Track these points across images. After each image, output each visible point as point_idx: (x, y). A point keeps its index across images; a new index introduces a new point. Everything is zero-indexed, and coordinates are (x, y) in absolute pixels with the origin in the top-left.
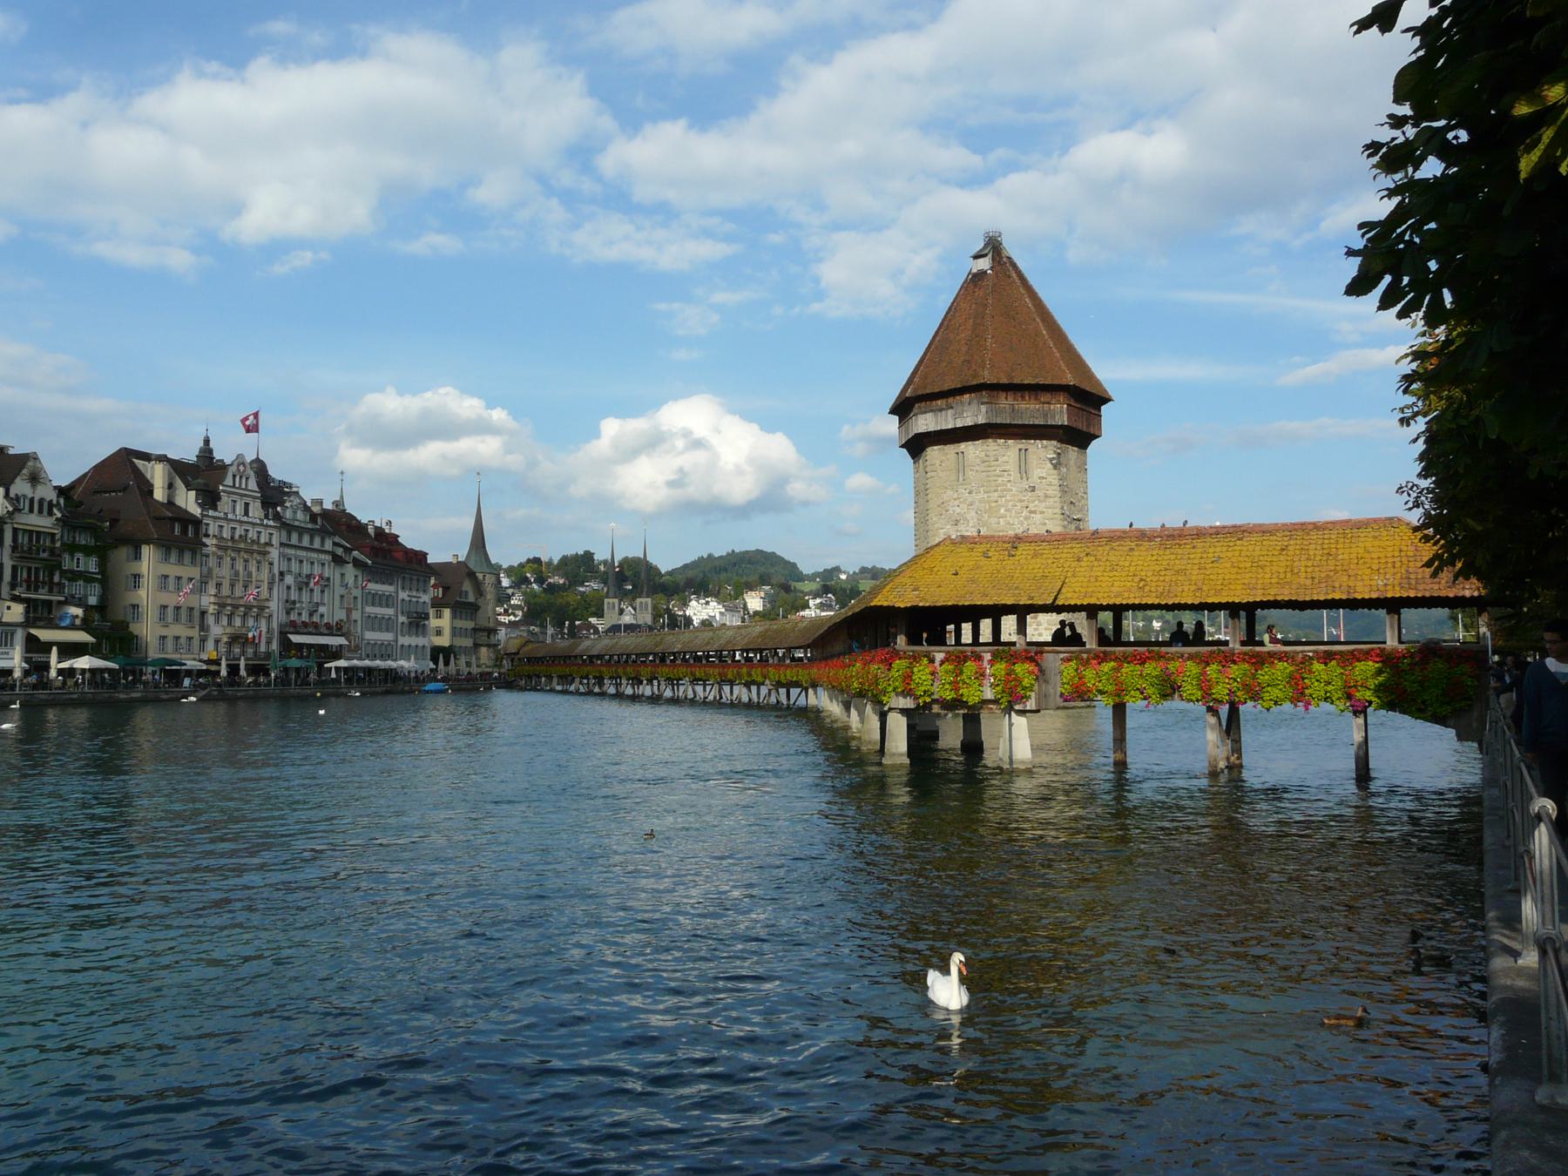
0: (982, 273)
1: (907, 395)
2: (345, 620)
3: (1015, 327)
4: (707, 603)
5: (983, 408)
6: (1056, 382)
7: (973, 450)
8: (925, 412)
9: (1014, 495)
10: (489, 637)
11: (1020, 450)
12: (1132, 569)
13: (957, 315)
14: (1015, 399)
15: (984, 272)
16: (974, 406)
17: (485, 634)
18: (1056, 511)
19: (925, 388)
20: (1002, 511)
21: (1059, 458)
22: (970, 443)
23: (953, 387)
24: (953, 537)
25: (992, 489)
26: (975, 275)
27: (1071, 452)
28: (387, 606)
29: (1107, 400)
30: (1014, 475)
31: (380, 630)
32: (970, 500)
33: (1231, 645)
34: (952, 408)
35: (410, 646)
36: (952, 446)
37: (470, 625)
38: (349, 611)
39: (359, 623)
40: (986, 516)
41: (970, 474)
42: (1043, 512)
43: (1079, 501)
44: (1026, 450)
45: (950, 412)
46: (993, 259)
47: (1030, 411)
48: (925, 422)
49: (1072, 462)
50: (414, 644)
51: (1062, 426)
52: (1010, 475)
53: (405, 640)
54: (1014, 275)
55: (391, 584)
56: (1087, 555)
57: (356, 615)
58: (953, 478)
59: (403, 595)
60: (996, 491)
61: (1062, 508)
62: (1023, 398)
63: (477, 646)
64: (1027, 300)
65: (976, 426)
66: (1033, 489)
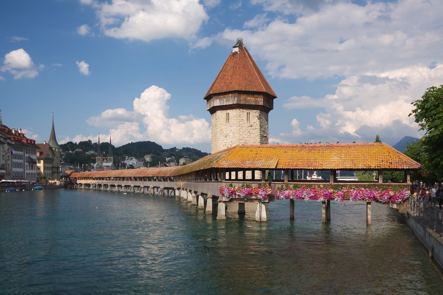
2: (5, 163)
4: (132, 159)
6: (260, 91)
7: (232, 113)
9: (245, 128)
10: (57, 170)
11: (247, 113)
12: (300, 157)
14: (246, 96)
17: (56, 169)
20: (241, 133)
23: (226, 91)
24: (240, 145)
28: (21, 159)
29: (275, 97)
31: (18, 167)
35: (29, 173)
37: (50, 166)
38: (6, 161)
39: (10, 165)
40: (236, 134)
42: (255, 134)
44: (249, 113)
45: (225, 99)
47: (251, 100)
48: (217, 102)
50: (31, 172)
52: (244, 121)
53: (28, 171)
55: (22, 151)
56: (285, 152)
57: (9, 162)
58: (225, 121)
59: (27, 155)
62: (249, 96)
63: (53, 173)
65: (233, 104)
66: (252, 126)
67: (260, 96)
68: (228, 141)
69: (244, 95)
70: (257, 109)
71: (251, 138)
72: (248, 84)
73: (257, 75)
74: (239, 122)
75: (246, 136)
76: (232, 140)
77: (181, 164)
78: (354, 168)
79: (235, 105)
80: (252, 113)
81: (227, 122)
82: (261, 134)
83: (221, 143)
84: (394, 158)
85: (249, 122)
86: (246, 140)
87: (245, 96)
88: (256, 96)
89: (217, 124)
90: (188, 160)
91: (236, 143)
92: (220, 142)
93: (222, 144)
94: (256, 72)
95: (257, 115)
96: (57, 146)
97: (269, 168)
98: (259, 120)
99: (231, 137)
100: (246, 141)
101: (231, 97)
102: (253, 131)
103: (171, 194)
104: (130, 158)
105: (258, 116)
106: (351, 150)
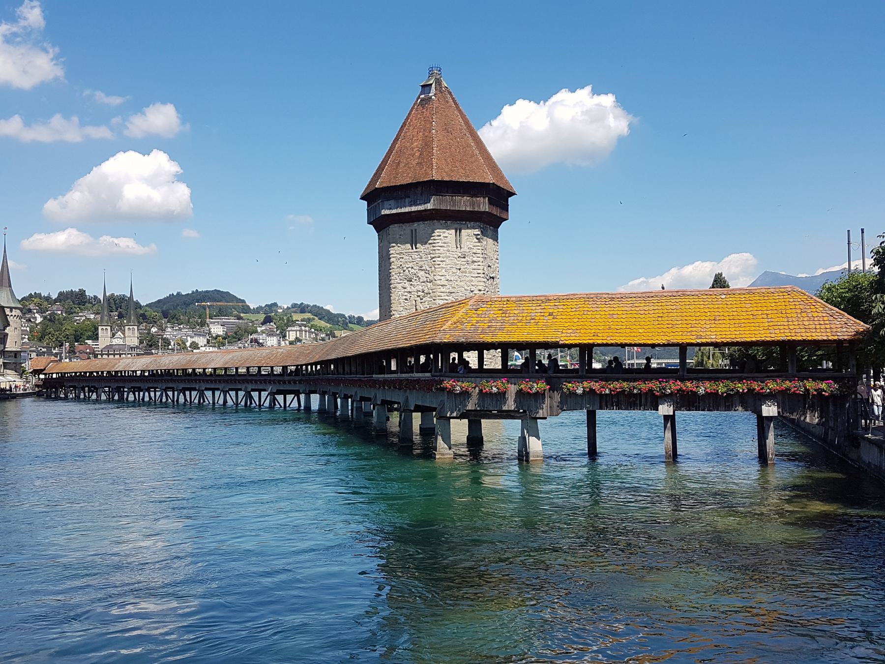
4: (180, 329)
6: (481, 181)
18: (479, 271)
22: (421, 222)
23: (410, 181)
26: (422, 100)
27: (489, 231)
34: (409, 197)
36: (408, 225)
40: (432, 275)
42: (472, 272)
43: (494, 265)
51: (484, 212)
52: (449, 246)
60: (439, 257)
64: (461, 120)
68: (415, 289)
74: (439, 248)
77: (291, 340)
79: (428, 212)
81: (412, 249)
82: (484, 274)
90: (306, 331)
95: (475, 233)
96: (14, 301)
98: (479, 244)
100: (455, 288)
101: (421, 195)
102: (468, 267)
103: (291, 406)
105: (478, 235)
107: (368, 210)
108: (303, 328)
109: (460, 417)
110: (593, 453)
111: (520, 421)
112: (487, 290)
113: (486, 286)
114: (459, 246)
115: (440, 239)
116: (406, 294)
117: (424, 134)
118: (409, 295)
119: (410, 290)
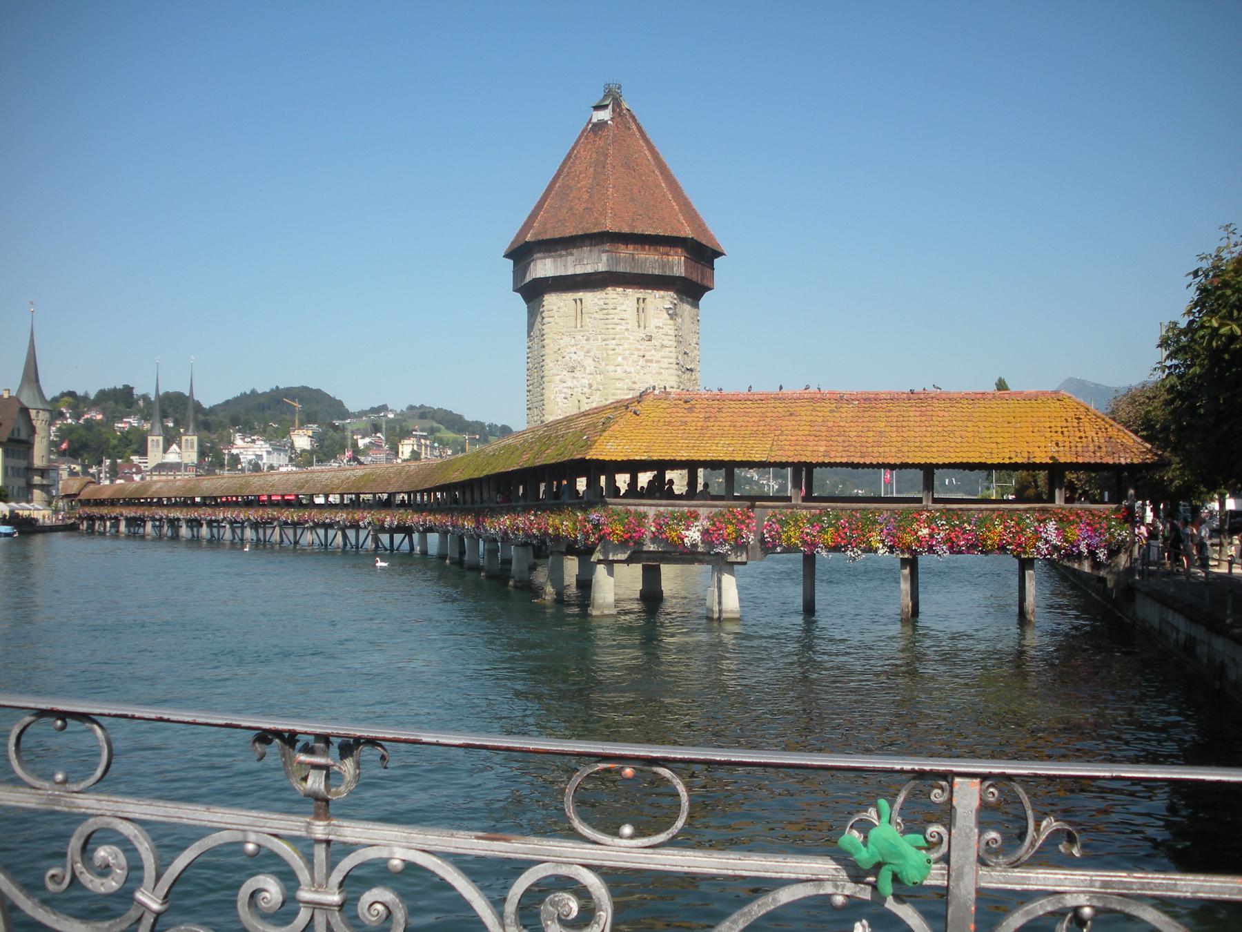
0: (602, 125)
1: (527, 240)
3: (634, 178)
4: (253, 441)
5: (604, 257)
6: (674, 234)
7: (591, 299)
8: (545, 258)
9: (631, 344)
11: (638, 299)
13: (577, 162)
14: (634, 249)
15: (606, 122)
16: (595, 255)
18: (671, 361)
19: (546, 232)
20: (620, 359)
21: (675, 308)
23: (574, 233)
25: (611, 336)
26: (595, 125)
29: (719, 254)
30: (632, 324)
32: (587, 347)
33: (924, 503)
34: (572, 254)
40: (603, 363)
41: (587, 320)
43: (692, 351)
44: (644, 299)
45: (570, 259)
46: (614, 111)
47: (649, 261)
48: (544, 268)
49: (686, 313)
51: (680, 278)
52: (628, 323)
54: (634, 127)
56: (791, 414)
58: (573, 324)
61: (677, 358)
62: (643, 249)
64: (647, 152)
65: (596, 273)
67: (675, 249)
68: (579, 385)
69: (627, 247)
70: (667, 289)
71: (650, 375)
72: (640, 212)
73: (665, 190)
74: (614, 326)
75: (633, 370)
76: (591, 381)
77: (403, 458)
78: (989, 462)
79: (599, 276)
80: (653, 299)
82: (678, 364)
83: (556, 389)
84: (1095, 435)
85: (642, 328)
86: (634, 379)
87: (631, 247)
88: (661, 249)
89: (544, 332)
90: (426, 446)
91: (604, 388)
92: (553, 385)
93: (561, 392)
94: (663, 179)
95: (666, 306)
97: (750, 459)
99: (588, 372)
100: (634, 383)
104: (249, 440)
105: (670, 308)
106: (977, 410)
107: (514, 272)
108: (423, 441)
109: (628, 561)
110: (809, 609)
111: (711, 566)
112: (681, 387)
113: (680, 382)
114: (642, 324)
115: (616, 314)
116: (565, 390)
117: (595, 170)
118: (570, 393)
119: (572, 386)
